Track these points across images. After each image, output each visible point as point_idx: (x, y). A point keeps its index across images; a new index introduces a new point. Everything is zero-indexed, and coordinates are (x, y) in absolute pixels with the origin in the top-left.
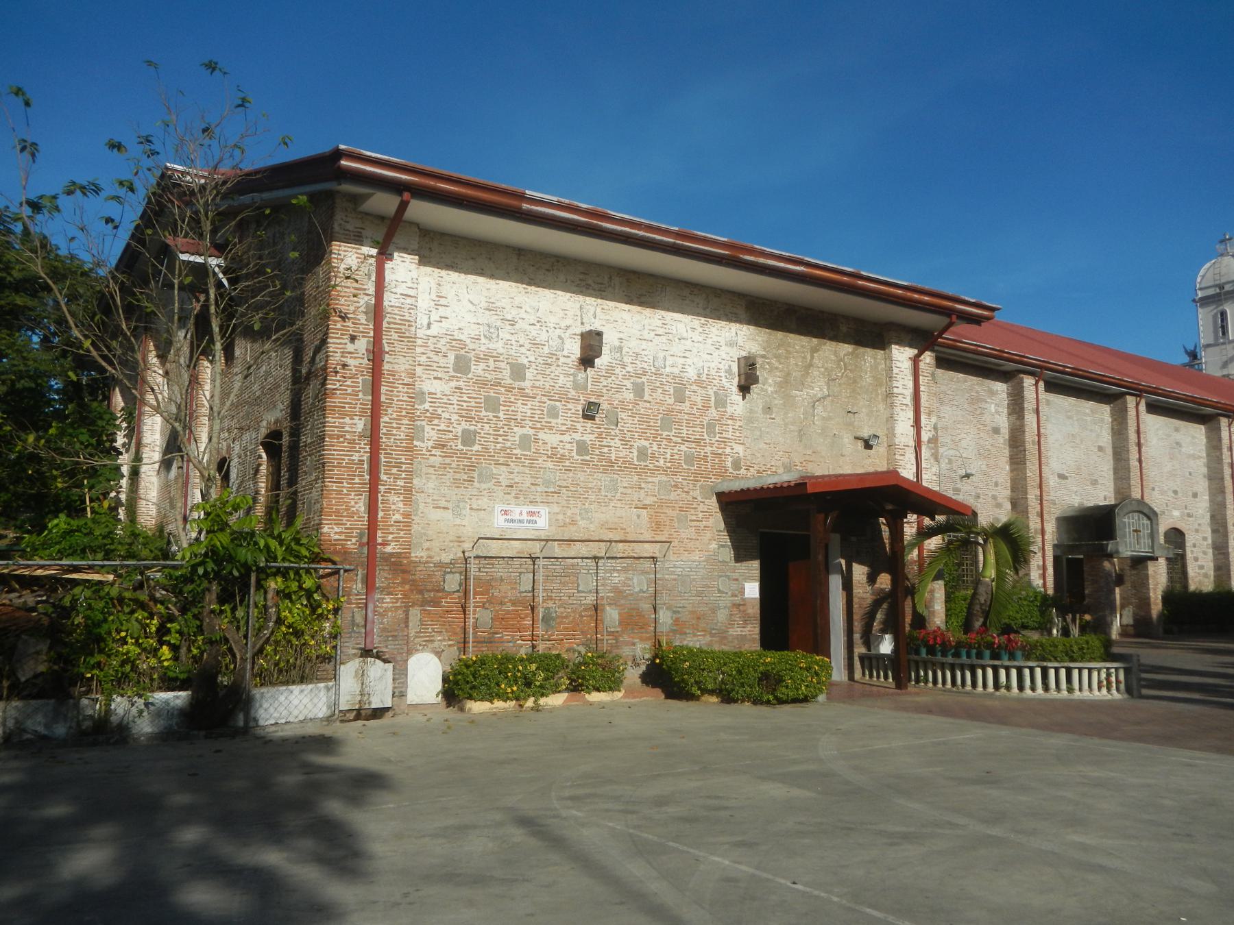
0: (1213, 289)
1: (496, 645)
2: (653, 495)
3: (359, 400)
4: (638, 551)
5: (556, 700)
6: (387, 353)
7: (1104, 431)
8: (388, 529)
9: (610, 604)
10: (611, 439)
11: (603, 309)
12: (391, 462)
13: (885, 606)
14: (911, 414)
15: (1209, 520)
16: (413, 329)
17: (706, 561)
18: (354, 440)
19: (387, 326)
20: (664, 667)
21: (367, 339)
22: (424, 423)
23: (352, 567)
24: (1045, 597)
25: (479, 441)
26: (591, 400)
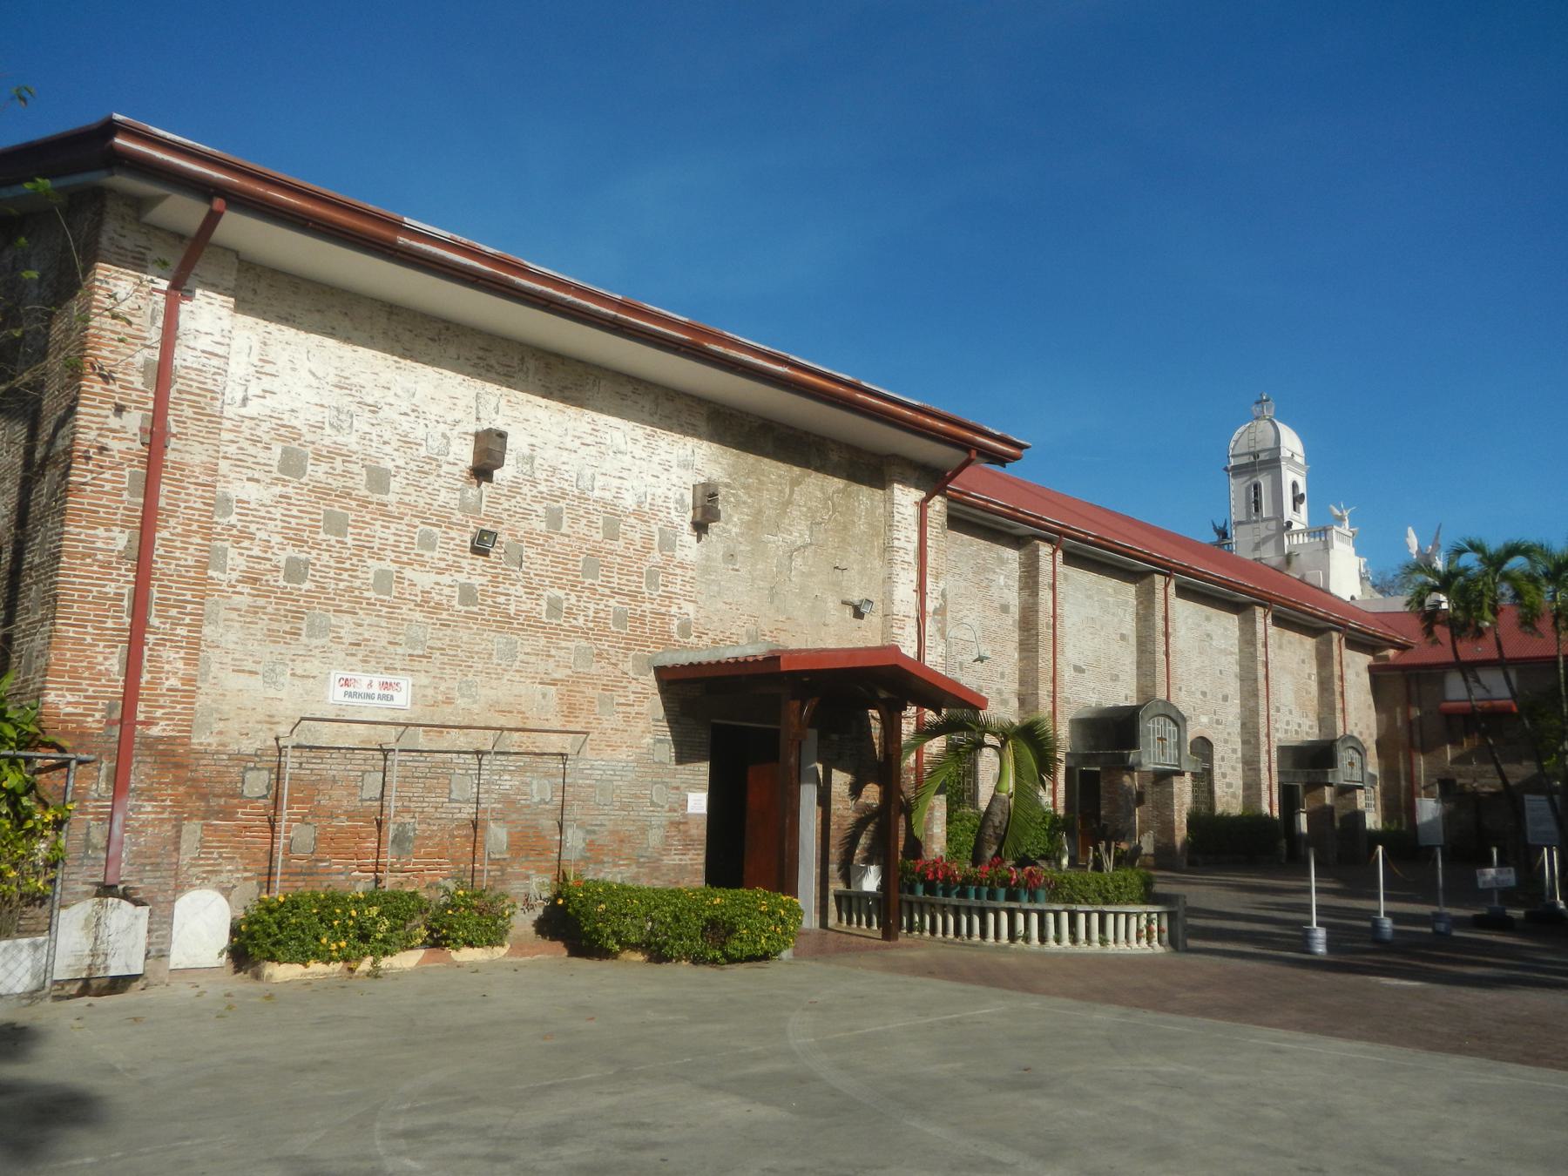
0: (1247, 457)
1: (322, 878)
2: (566, 667)
3: (122, 502)
4: (541, 745)
5: (406, 960)
6: (174, 435)
8: (156, 701)
9: (495, 820)
10: (511, 584)
11: (509, 401)
12: (169, 599)
13: (871, 827)
14: (914, 576)
15: (1239, 729)
16: (218, 403)
17: (637, 761)
18: (111, 562)
19: (177, 395)
20: (570, 910)
21: (142, 412)
22: (227, 544)
23: (92, 757)
24: (1055, 818)
25: (312, 575)
26: (486, 528)
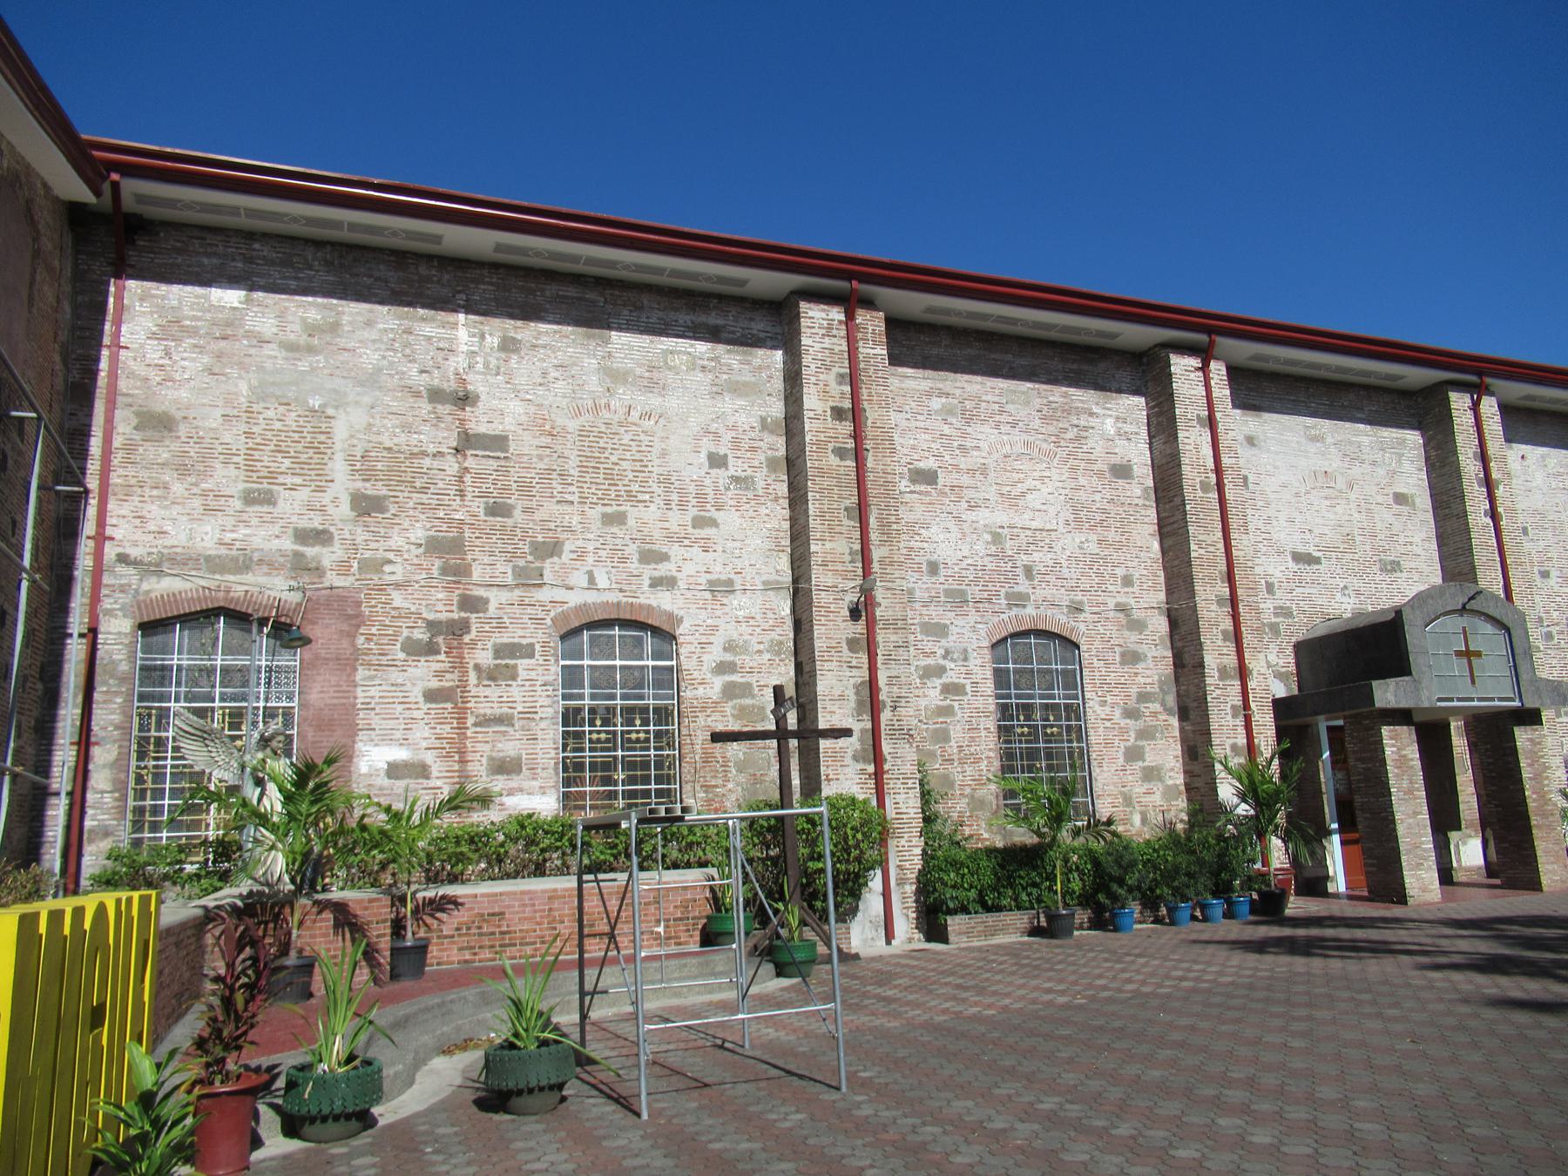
7: (1407, 466)
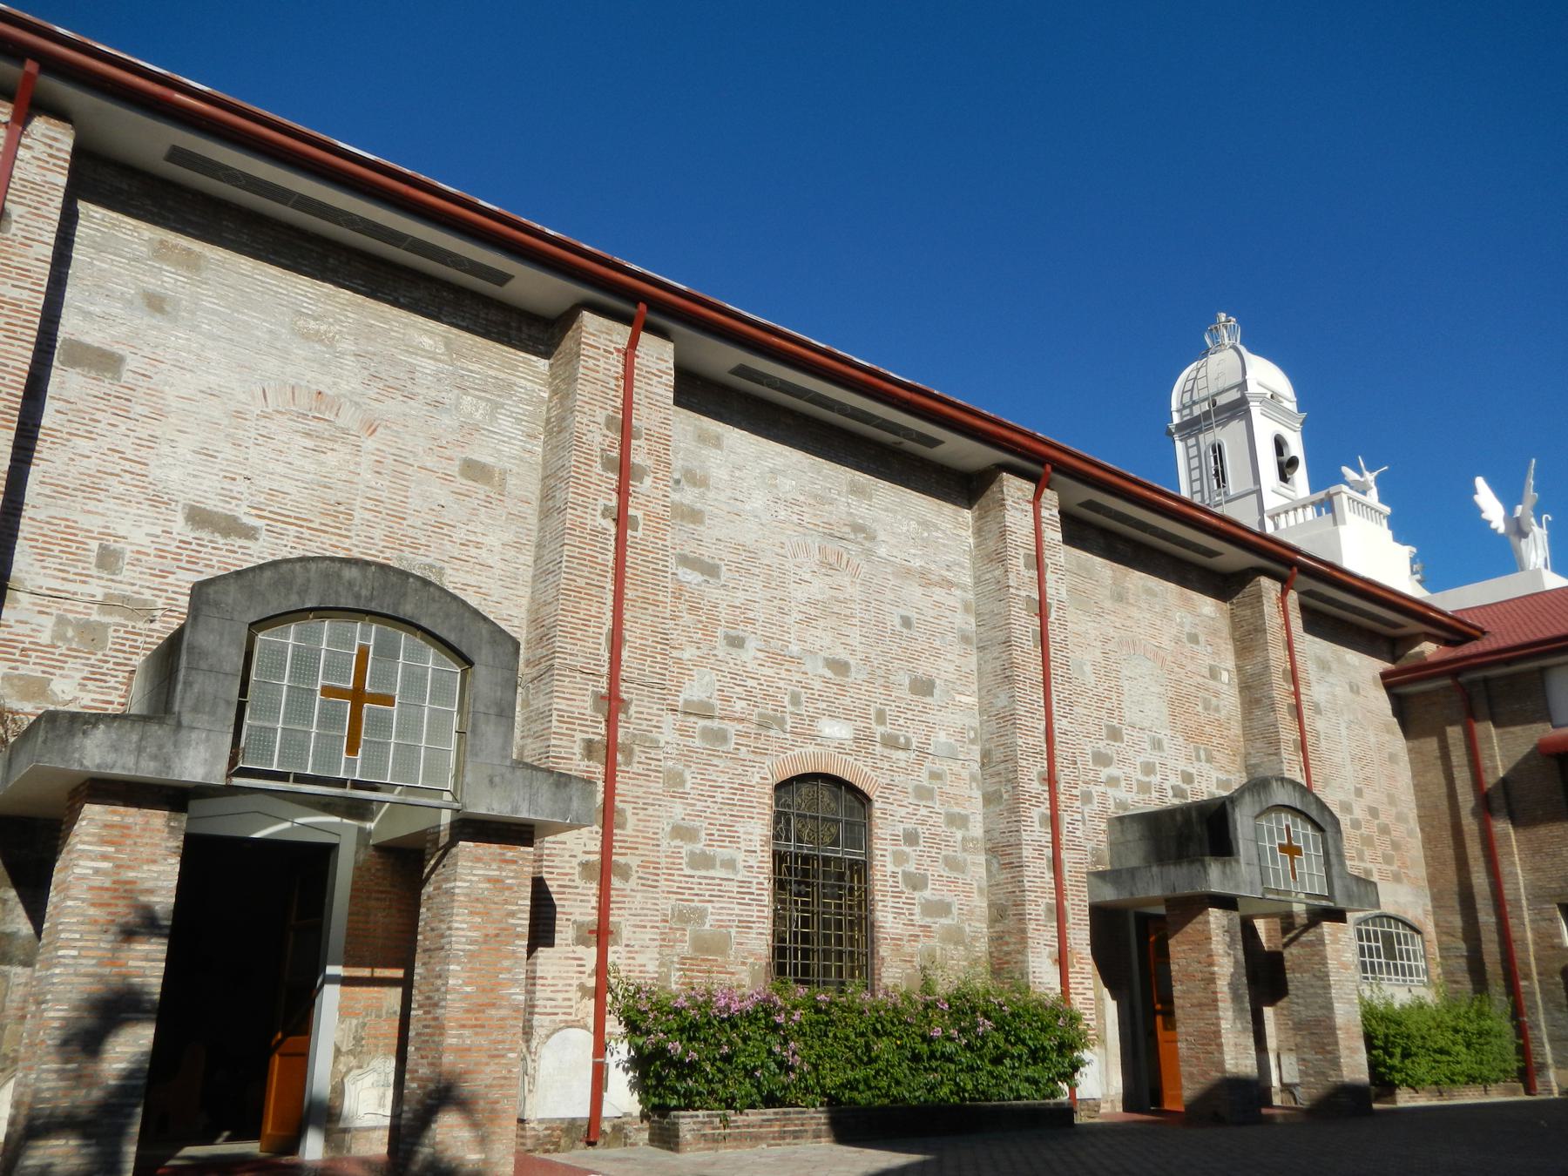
7: (505, 423)
15: (976, 767)
